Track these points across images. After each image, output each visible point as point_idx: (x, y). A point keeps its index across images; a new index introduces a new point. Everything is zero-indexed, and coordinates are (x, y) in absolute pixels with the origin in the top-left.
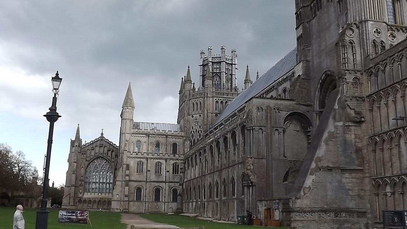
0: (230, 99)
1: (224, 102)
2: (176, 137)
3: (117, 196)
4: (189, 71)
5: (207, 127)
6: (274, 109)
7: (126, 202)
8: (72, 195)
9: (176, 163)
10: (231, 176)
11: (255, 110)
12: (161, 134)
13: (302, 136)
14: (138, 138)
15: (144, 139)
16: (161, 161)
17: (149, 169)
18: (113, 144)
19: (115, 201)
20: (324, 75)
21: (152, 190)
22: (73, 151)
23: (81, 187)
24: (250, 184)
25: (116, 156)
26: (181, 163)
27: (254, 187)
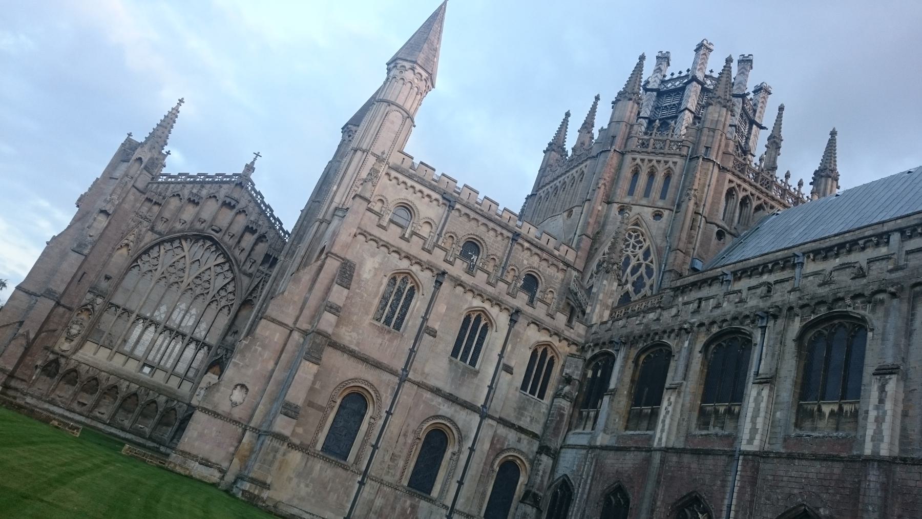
0: (773, 203)
1: (755, 203)
2: (545, 256)
3: (237, 395)
5: (684, 263)
7: (276, 443)
8: (31, 329)
9: (547, 346)
12: (497, 219)
16: (494, 311)
17: (434, 323)
18: (272, 215)
19: (216, 415)
21: (414, 425)
22: (118, 174)
23: (84, 316)
25: (270, 260)
26: (572, 355)
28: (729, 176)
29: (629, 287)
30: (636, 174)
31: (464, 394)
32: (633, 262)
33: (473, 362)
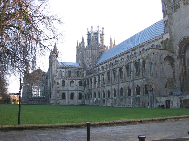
4: (83, 37)
6: (160, 54)
10: (127, 86)
11: (152, 55)
13: (170, 66)
14: (60, 70)
15: (63, 70)
17: (68, 84)
20: (183, 39)
24: (152, 89)
27: (154, 91)
28: (97, 50)
29: (89, 69)
30: (86, 53)
31: (73, 89)
32: (89, 65)
33: (73, 86)
